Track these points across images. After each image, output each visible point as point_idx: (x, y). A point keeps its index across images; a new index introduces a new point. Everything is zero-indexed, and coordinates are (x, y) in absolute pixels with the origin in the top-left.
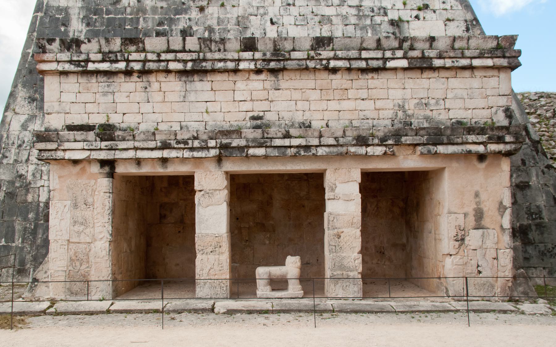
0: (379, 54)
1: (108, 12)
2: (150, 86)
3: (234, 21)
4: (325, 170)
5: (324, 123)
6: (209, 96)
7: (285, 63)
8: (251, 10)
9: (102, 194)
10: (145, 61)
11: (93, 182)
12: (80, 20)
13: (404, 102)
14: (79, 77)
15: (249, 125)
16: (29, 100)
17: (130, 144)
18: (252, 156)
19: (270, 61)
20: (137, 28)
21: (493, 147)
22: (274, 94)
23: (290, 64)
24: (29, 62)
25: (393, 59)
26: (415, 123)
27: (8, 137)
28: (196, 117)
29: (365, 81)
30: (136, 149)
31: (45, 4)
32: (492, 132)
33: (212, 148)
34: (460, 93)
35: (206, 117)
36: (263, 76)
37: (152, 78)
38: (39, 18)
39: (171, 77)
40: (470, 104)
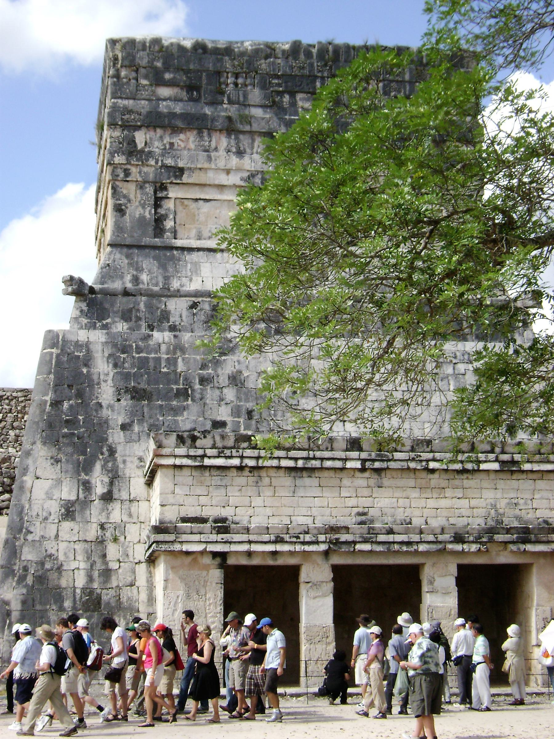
1: (139, 350)
2: (261, 481)
4: (423, 564)
5: (423, 520)
6: (317, 492)
7: (389, 463)
9: (214, 584)
10: (258, 458)
11: (204, 573)
12: (105, 359)
13: (496, 502)
14: (193, 470)
15: (354, 520)
16: (52, 461)
17: (245, 537)
18: (359, 551)
19: (373, 461)
20: (175, 371)
23: (392, 465)
24: (48, 413)
25: (485, 462)
26: (506, 520)
28: (304, 511)
29: (461, 481)
30: (250, 542)
31: (61, 337)
33: (322, 542)
35: (315, 512)
36: (367, 474)
37: (263, 473)
38: (54, 355)
39: (281, 473)
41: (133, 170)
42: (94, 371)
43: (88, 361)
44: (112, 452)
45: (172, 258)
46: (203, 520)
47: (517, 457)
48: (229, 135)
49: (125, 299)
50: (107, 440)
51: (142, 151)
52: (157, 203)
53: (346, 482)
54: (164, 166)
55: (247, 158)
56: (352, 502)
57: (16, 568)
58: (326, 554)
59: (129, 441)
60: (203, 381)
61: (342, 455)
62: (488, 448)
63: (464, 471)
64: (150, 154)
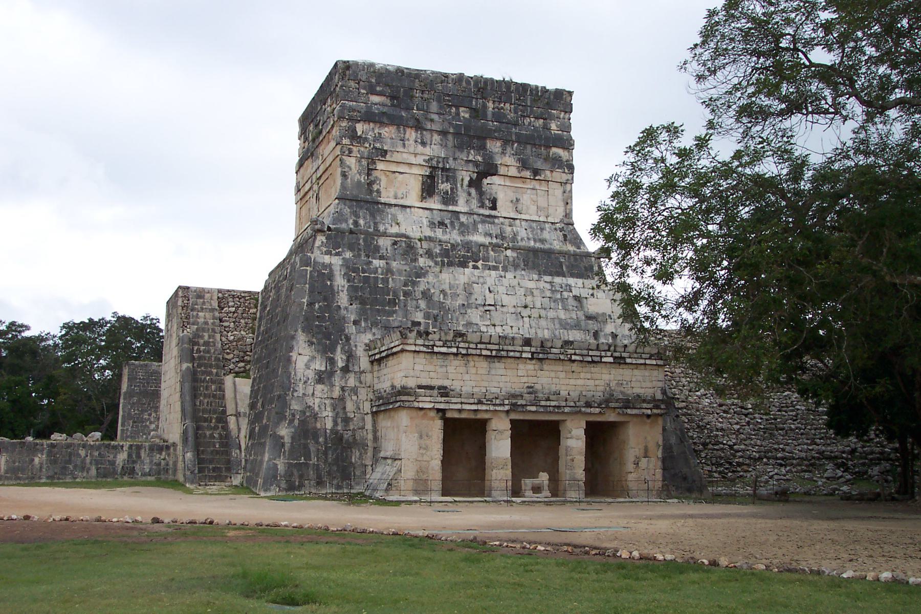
0: (598, 353)
3: (461, 287)
4: (564, 421)
6: (502, 372)
8: (474, 279)
17: (459, 400)
21: (655, 411)
22: (540, 373)
23: (550, 356)
27: (295, 374)
30: (462, 403)
32: (656, 403)
34: (640, 378)
35: (501, 385)
36: (534, 362)
37: (470, 358)
40: (644, 385)
41: (355, 149)
42: (336, 284)
43: (331, 277)
44: (348, 339)
45: (378, 210)
46: (431, 388)
47: (624, 355)
48: (416, 131)
49: (351, 236)
50: (344, 330)
51: (360, 137)
52: (369, 172)
53: (521, 366)
54: (374, 148)
55: (428, 147)
56: (525, 379)
57: (287, 414)
58: (507, 412)
59: (359, 332)
60: (406, 294)
61: (520, 349)
62: (607, 348)
63: (593, 362)
64: (366, 139)
